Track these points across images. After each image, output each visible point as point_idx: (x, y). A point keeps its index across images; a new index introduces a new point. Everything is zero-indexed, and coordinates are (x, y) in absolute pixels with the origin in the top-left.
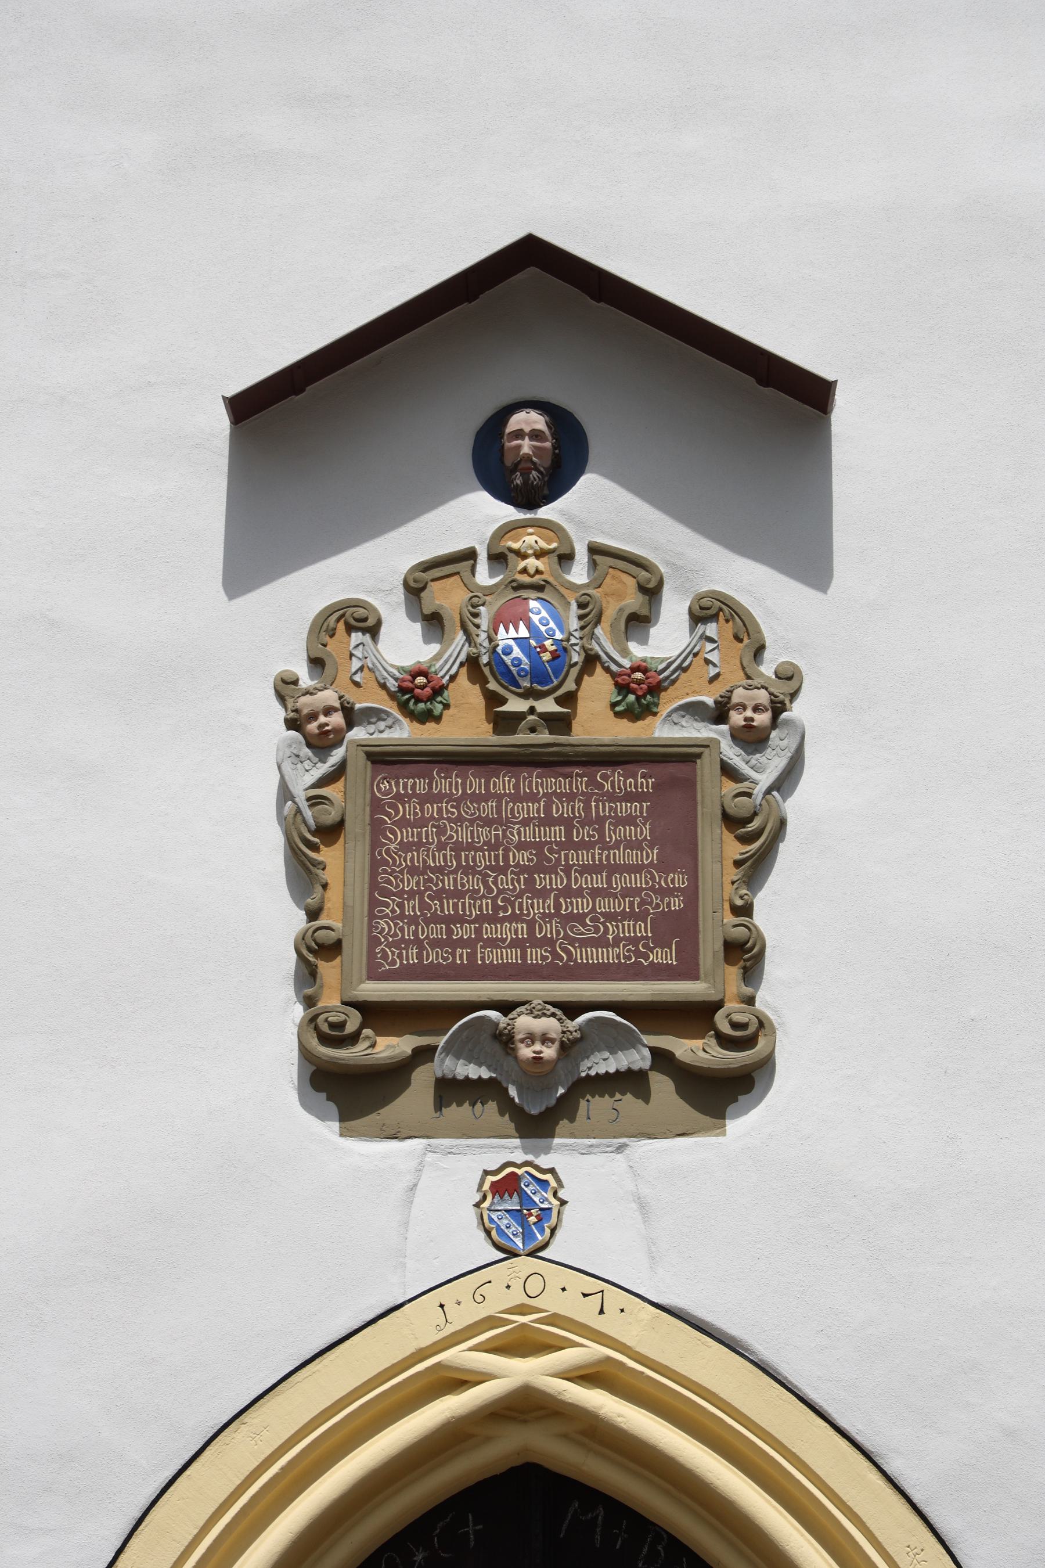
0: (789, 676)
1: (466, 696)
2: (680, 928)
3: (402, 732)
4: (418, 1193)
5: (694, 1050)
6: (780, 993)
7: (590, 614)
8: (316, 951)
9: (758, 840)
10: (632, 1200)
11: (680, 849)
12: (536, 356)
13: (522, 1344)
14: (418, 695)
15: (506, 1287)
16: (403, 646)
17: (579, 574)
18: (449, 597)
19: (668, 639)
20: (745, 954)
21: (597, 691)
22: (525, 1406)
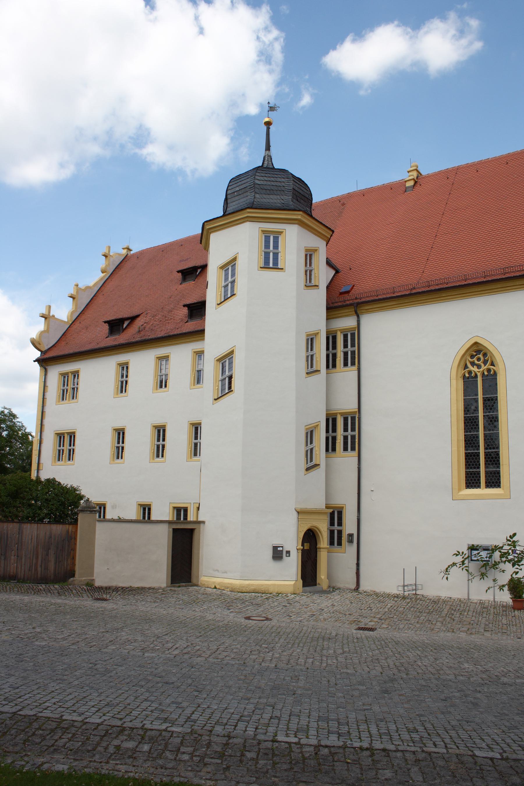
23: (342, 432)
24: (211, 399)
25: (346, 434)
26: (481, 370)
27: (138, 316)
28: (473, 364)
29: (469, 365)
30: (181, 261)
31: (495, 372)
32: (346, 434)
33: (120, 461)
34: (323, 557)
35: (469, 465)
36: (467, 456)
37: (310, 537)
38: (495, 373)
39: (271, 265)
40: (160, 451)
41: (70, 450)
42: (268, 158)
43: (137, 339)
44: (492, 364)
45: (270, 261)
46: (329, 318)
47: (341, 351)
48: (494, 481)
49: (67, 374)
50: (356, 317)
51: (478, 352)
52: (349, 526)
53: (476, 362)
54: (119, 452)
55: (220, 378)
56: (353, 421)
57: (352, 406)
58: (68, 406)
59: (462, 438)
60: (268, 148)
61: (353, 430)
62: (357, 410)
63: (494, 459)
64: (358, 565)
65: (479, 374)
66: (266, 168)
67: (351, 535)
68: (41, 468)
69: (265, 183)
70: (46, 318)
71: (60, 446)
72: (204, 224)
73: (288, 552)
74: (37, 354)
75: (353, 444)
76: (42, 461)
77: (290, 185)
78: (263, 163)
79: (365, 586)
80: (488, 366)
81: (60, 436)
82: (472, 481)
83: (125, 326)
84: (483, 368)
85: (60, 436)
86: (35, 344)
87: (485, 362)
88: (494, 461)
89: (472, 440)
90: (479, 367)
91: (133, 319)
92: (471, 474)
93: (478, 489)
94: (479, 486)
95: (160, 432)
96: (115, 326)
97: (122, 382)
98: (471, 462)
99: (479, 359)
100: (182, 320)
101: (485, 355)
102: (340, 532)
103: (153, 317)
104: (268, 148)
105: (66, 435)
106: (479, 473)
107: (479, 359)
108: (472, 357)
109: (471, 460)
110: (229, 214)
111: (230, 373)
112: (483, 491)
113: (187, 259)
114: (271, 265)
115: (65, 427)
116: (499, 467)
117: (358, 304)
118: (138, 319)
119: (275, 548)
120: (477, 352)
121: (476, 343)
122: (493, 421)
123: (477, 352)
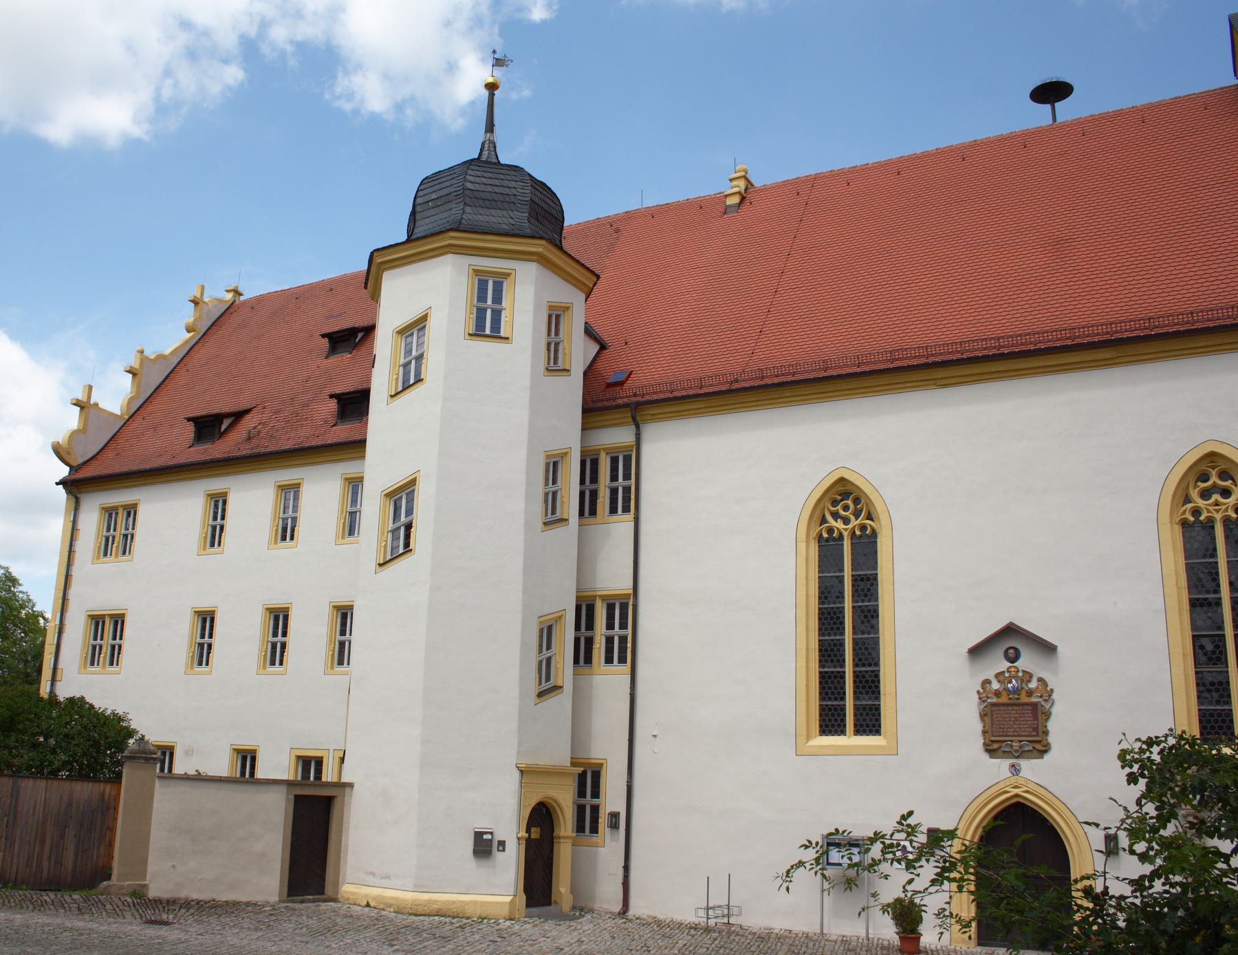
0: (1052, 690)
1: (1004, 693)
2: (1036, 729)
3: (994, 700)
4: (1001, 766)
5: (1038, 746)
6: (1051, 739)
7: (1022, 681)
8: (984, 732)
9: (1048, 715)
10: (1031, 769)
11: (1036, 718)
13: (1016, 787)
14: (997, 694)
15: (1013, 780)
16: (996, 685)
17: (1020, 674)
18: (1001, 678)
19: (1033, 685)
20: (1046, 733)
21: (1024, 693)
22: (1017, 795)
23: (600, 629)
24: (373, 565)
25: (610, 633)
26: (850, 526)
27: (247, 411)
28: (836, 516)
30: (328, 317)
31: (873, 531)
33: (203, 669)
34: (564, 853)
35: (827, 693)
36: (823, 677)
37: (541, 817)
38: (874, 534)
39: (488, 331)
40: (276, 654)
41: (113, 647)
42: (490, 146)
43: (244, 452)
44: (869, 517)
45: (487, 324)
46: (585, 428)
47: (602, 486)
48: (869, 723)
49: (115, 509)
50: (633, 427)
51: (845, 495)
52: (612, 799)
53: (842, 513)
54: (203, 654)
55: (391, 526)
56: (623, 609)
57: (625, 586)
58: (113, 566)
59: (815, 645)
60: (490, 127)
61: (623, 626)
62: (631, 591)
63: (869, 684)
64: (626, 868)
65: (845, 534)
66: (486, 161)
67: (614, 816)
68: (58, 678)
69: (483, 188)
70: (82, 408)
71: (95, 639)
72: (372, 254)
73: (502, 844)
74: (64, 471)
75: (623, 651)
76: (61, 665)
77: (527, 192)
78: (480, 154)
79: (639, 907)
81: (97, 621)
82: (831, 723)
83: (223, 427)
84: (854, 522)
85: (97, 621)
86: (59, 451)
87: (857, 516)
88: (870, 687)
89: (832, 650)
90: (846, 521)
91: (238, 416)
92: (830, 710)
93: (842, 737)
94: (842, 732)
95: (279, 619)
96: (207, 427)
97: (214, 528)
98: (830, 688)
100: (326, 422)
101: (857, 501)
102: (595, 809)
103: (275, 413)
104: (490, 127)
105: (107, 620)
106: (843, 708)
108: (835, 503)
109: (830, 685)
110: (418, 239)
111: (409, 519)
112: (849, 740)
113: (341, 314)
114: (488, 331)
115: (106, 603)
116: (878, 698)
117: (638, 405)
118: (248, 417)
119: (478, 835)
120: (844, 495)
121: (842, 480)
122: (868, 617)
123: (844, 495)
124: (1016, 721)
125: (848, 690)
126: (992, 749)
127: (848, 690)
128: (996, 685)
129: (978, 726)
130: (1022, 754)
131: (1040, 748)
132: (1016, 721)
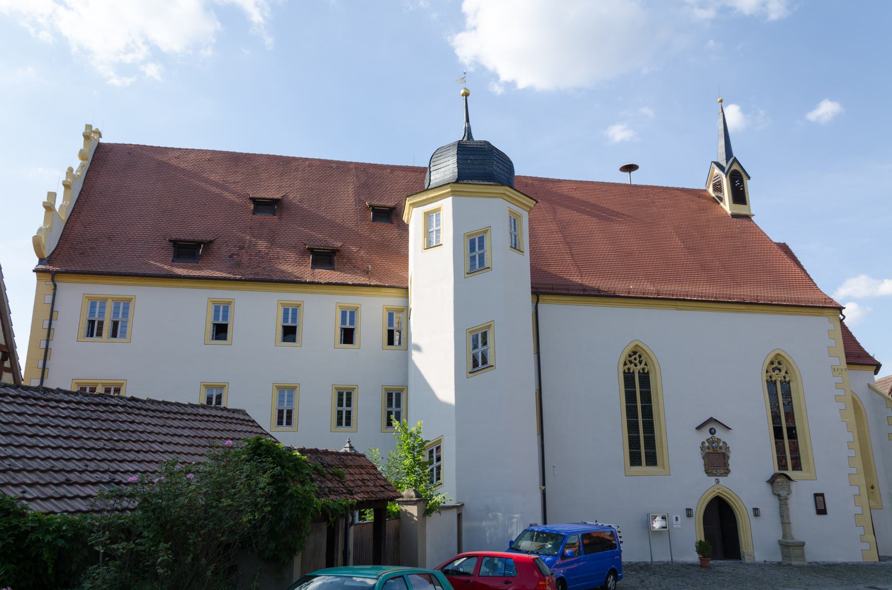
6: (730, 468)
12: (710, 424)
14: (708, 448)
19: (721, 444)
28: (631, 362)
29: (628, 362)
32: (348, 409)
42: (468, 132)
44: (646, 364)
48: (652, 460)
51: (635, 353)
60: (468, 120)
63: (651, 443)
80: (643, 365)
84: (640, 367)
90: (636, 365)
94: (640, 464)
99: (635, 359)
101: (640, 356)
104: (468, 120)
106: (640, 453)
107: (635, 359)
109: (633, 443)
112: (644, 469)
120: (635, 355)
124: (716, 460)
125: (643, 446)
126: (708, 472)
127: (643, 446)
128: (707, 444)
129: (702, 462)
130: (721, 475)
131: (727, 472)
132: (716, 460)
